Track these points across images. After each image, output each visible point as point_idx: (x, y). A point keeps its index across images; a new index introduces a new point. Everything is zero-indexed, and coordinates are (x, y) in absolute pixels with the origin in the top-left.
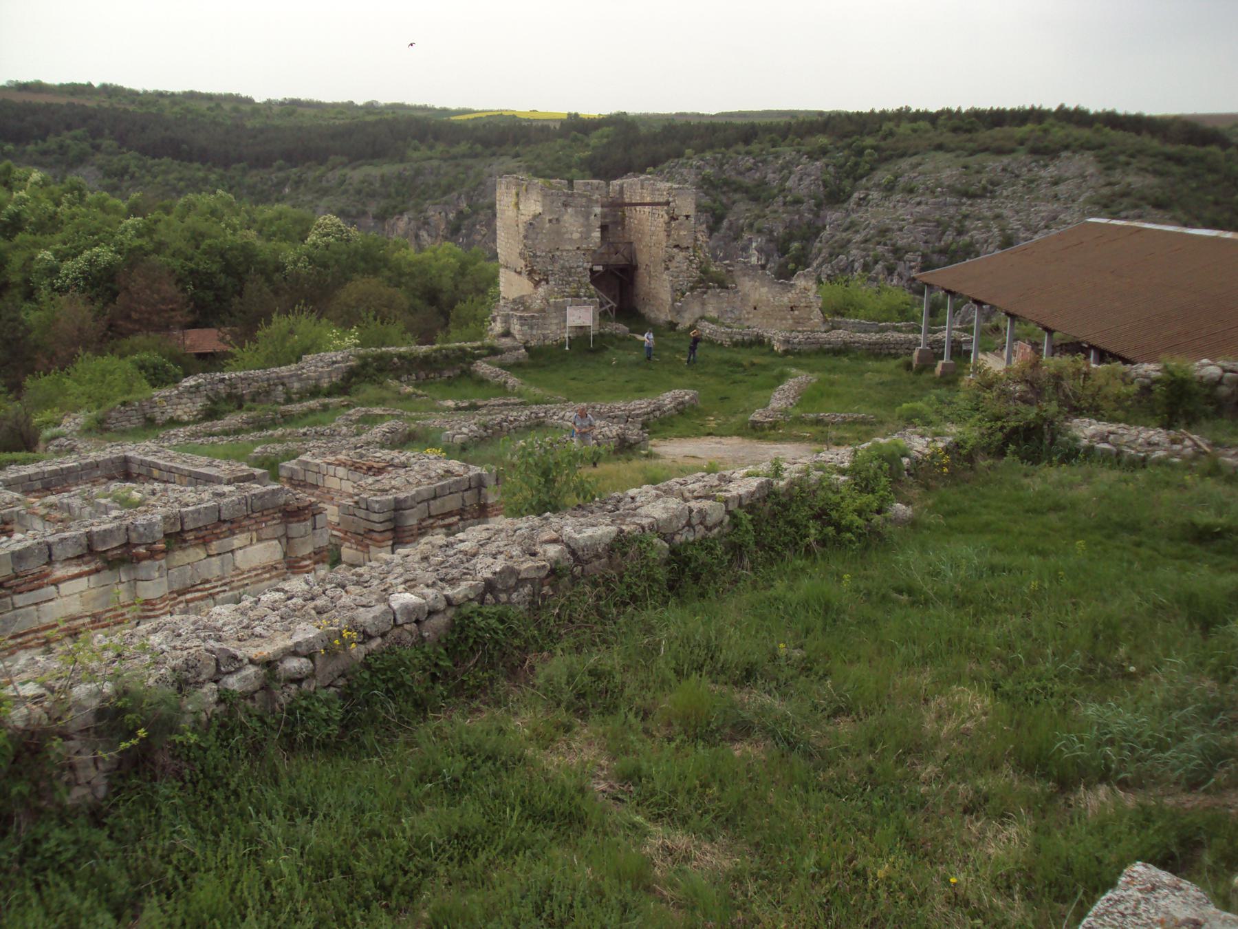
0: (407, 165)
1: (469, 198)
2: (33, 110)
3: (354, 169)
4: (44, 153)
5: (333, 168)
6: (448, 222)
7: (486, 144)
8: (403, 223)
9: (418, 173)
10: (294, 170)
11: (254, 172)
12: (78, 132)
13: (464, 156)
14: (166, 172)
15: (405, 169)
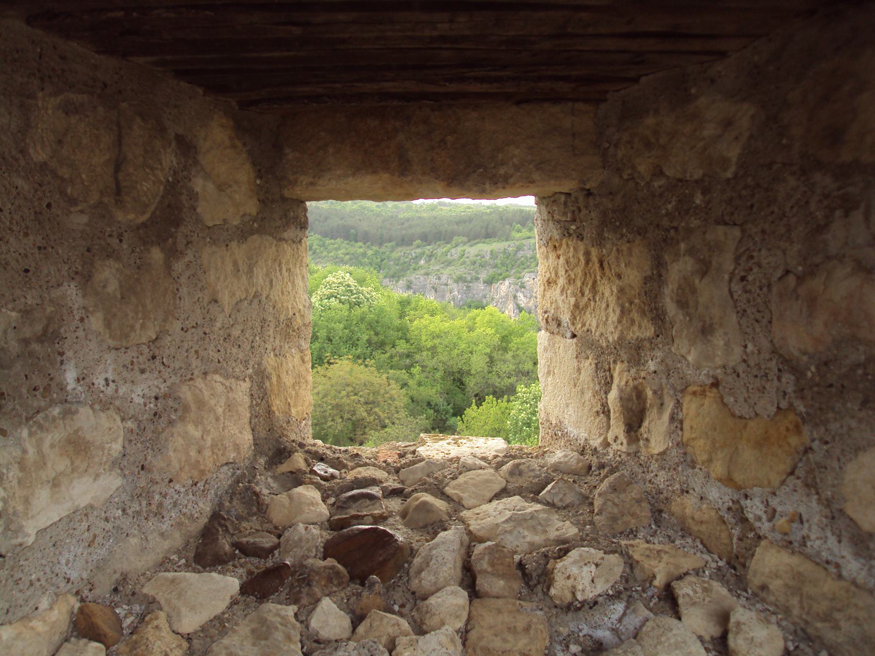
3: (471, 246)
9: (519, 249)
10: (428, 247)
11: (400, 249)
14: (337, 249)
15: (509, 246)
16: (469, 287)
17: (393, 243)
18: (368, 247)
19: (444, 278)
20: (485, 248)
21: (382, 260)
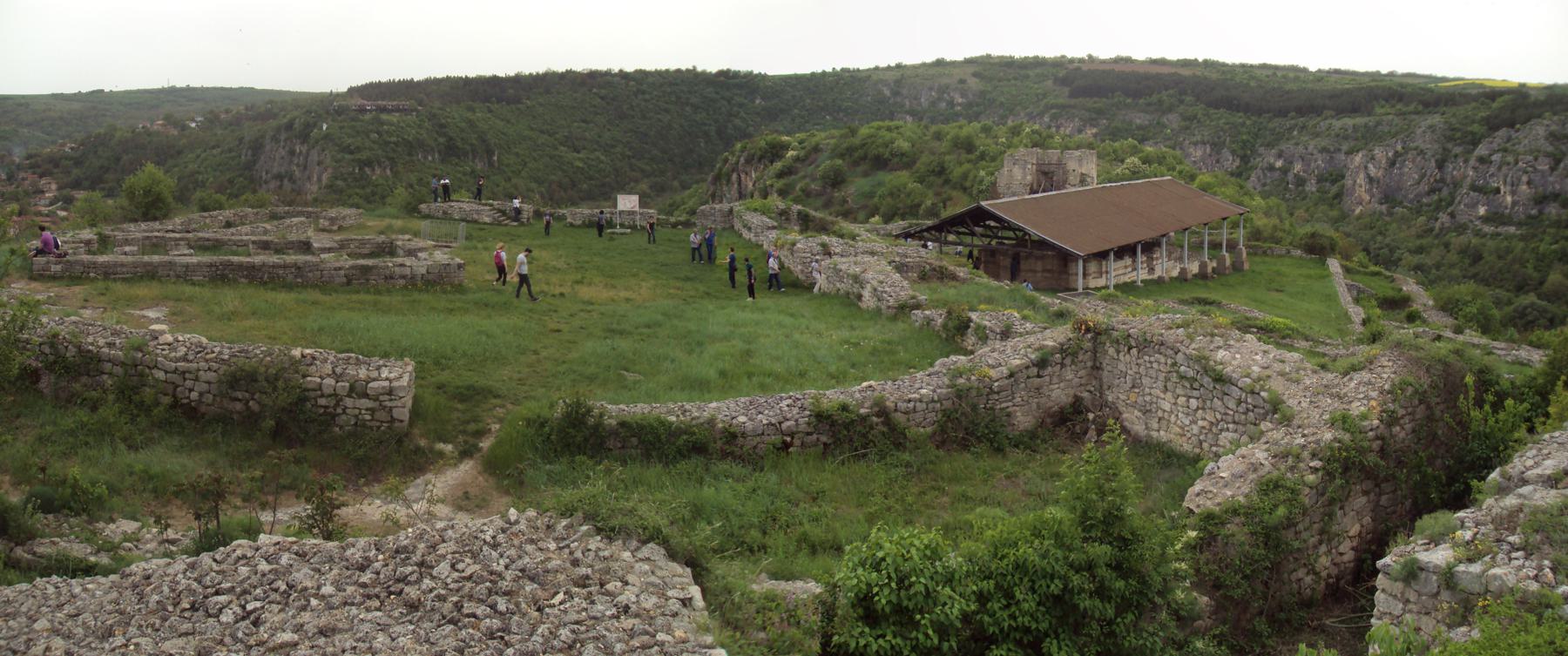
0: (1371, 118)
2: (1158, 77)
4: (1149, 104)
5: (1326, 119)
6: (1388, 159)
7: (1426, 105)
8: (1358, 158)
9: (1378, 124)
12: (1171, 92)
13: (1410, 113)
14: (1219, 119)
16: (1331, 157)
17: (1271, 115)
18: (1249, 118)
19: (1311, 148)
20: (1349, 122)
21: (1259, 130)
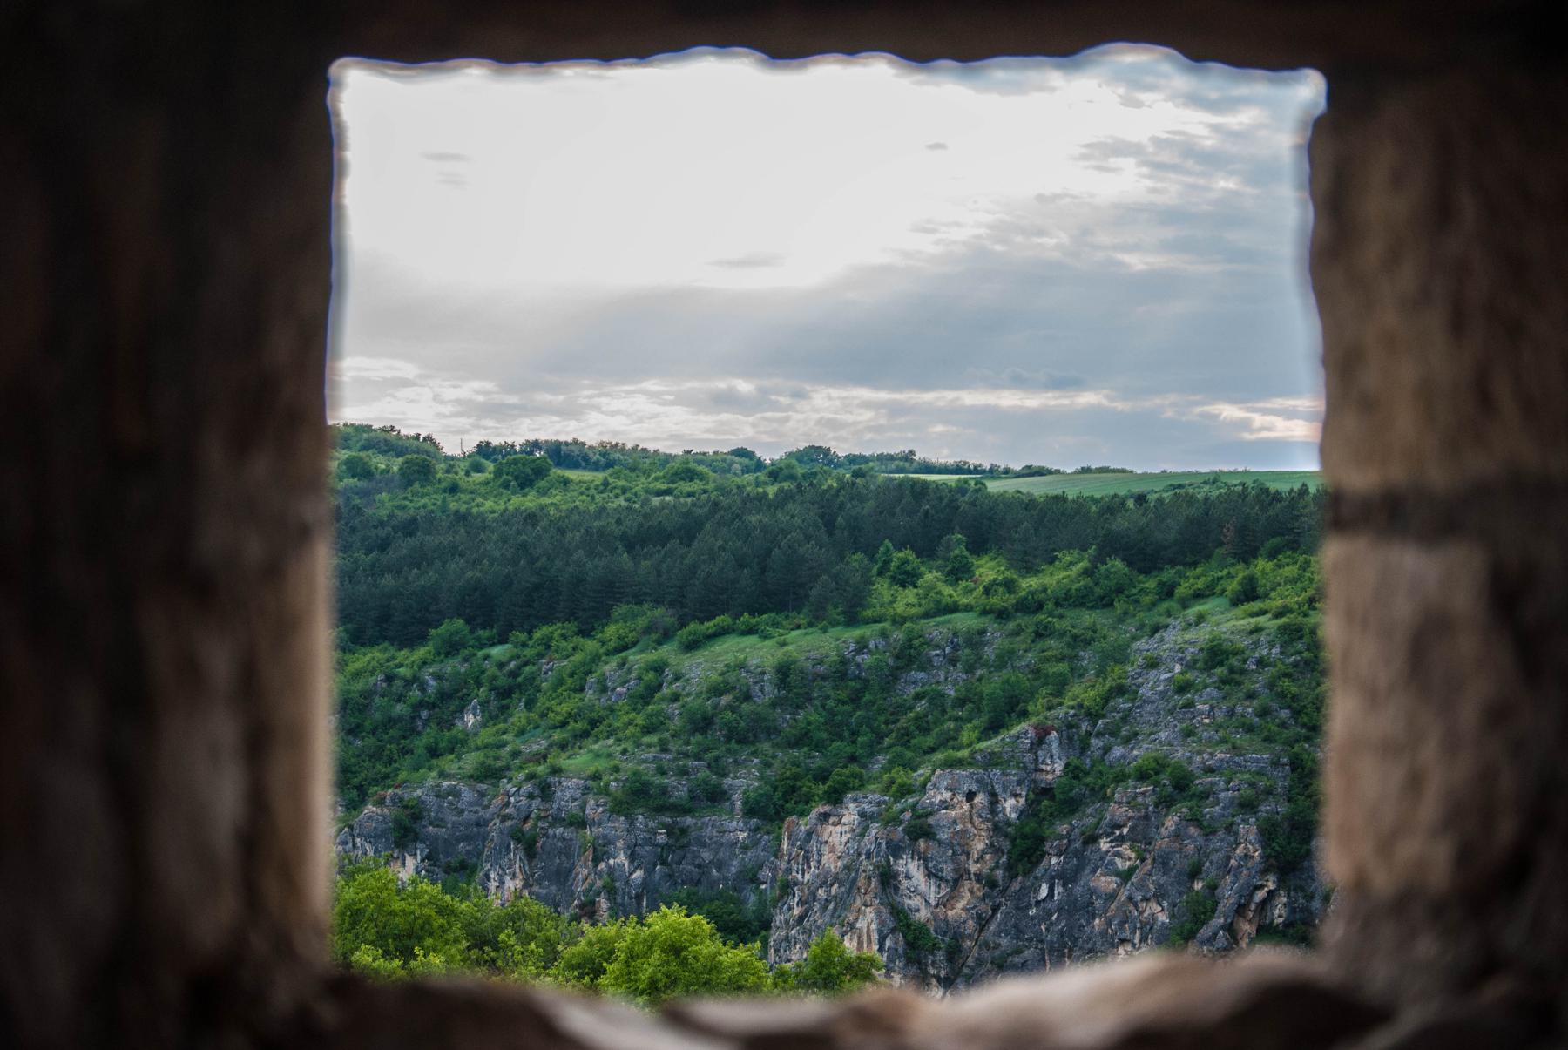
1: (1075, 741)
3: (692, 646)
7: (1145, 557)
9: (909, 656)
10: (497, 651)
15: (862, 646)
